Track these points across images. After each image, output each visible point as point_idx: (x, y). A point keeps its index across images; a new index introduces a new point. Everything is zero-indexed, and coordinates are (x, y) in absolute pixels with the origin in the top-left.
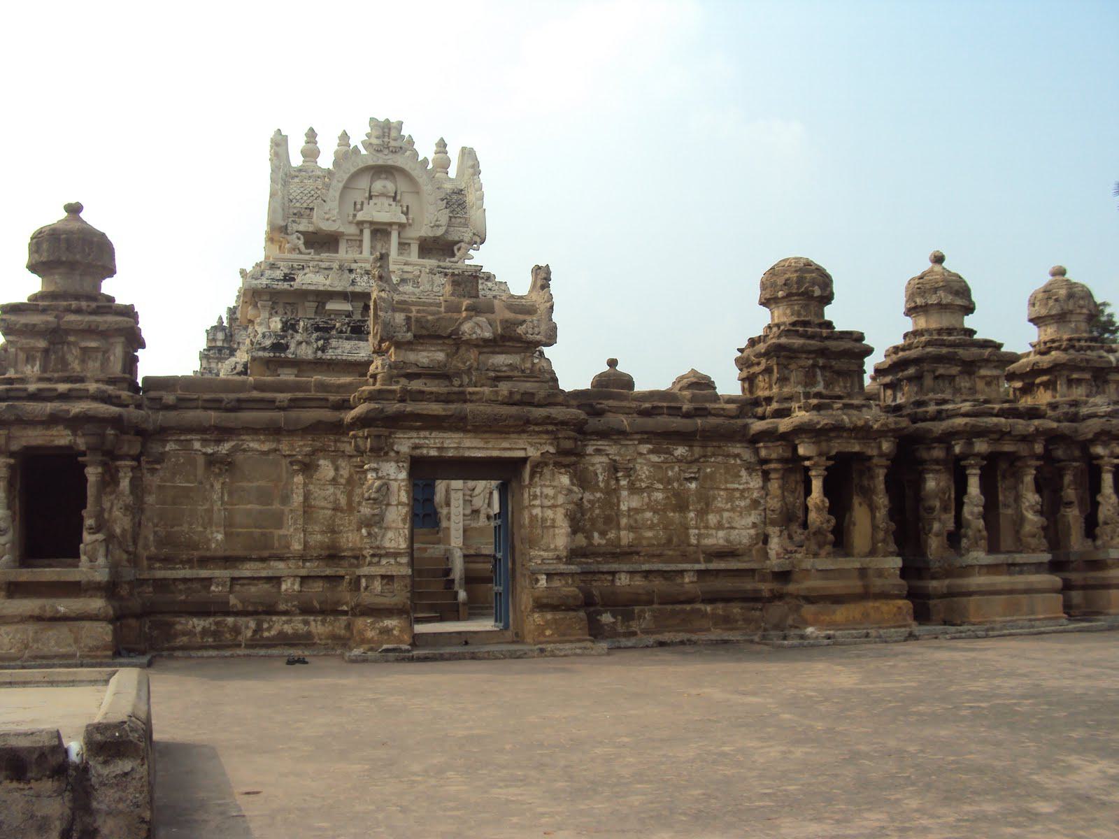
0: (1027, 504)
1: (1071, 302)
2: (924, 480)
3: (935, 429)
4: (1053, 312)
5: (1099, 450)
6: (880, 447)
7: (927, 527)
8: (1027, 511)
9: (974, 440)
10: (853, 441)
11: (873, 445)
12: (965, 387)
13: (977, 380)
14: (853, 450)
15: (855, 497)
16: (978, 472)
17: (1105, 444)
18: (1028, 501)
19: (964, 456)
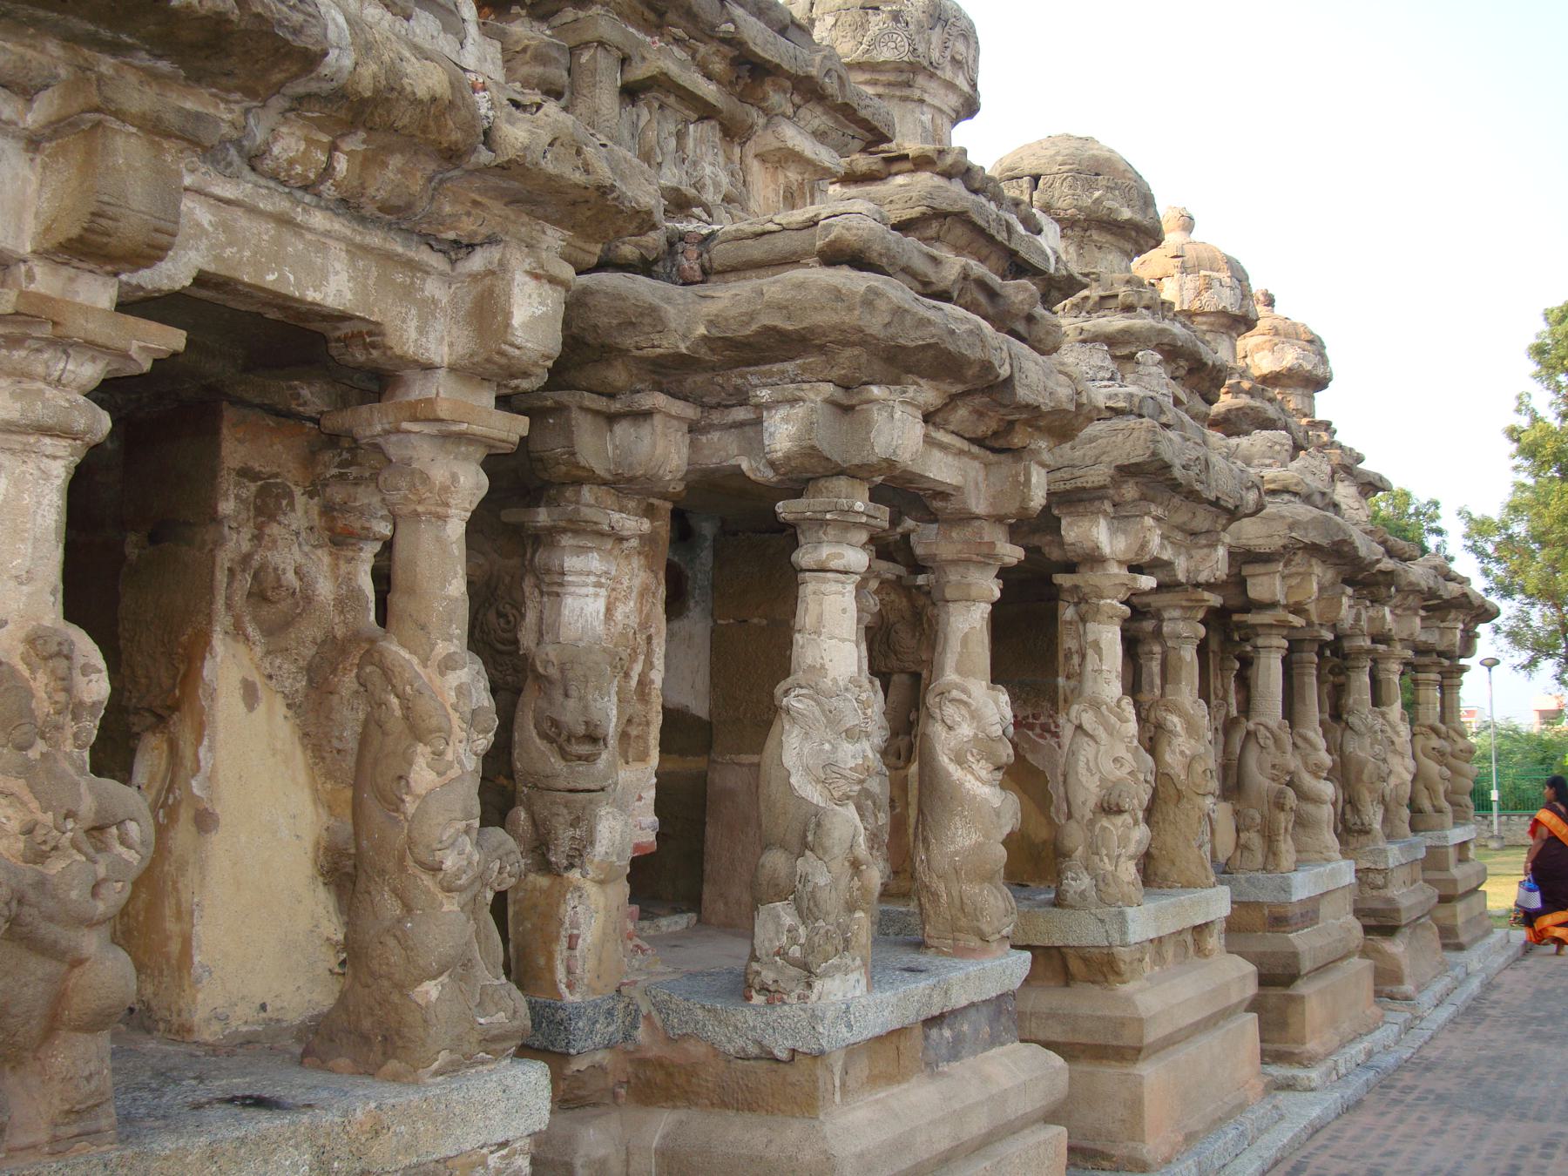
0: (966, 730)
1: (936, 36)
2: (552, 585)
3: (670, 311)
4: (885, 54)
5: (1099, 533)
6: (487, 311)
7: (565, 837)
8: (960, 760)
9: (875, 391)
10: (319, 220)
11: (433, 288)
12: (717, 185)
13: (755, 166)
14: (312, 295)
15: (220, 644)
16: (857, 558)
17: (1121, 516)
18: (975, 716)
19: (805, 474)
